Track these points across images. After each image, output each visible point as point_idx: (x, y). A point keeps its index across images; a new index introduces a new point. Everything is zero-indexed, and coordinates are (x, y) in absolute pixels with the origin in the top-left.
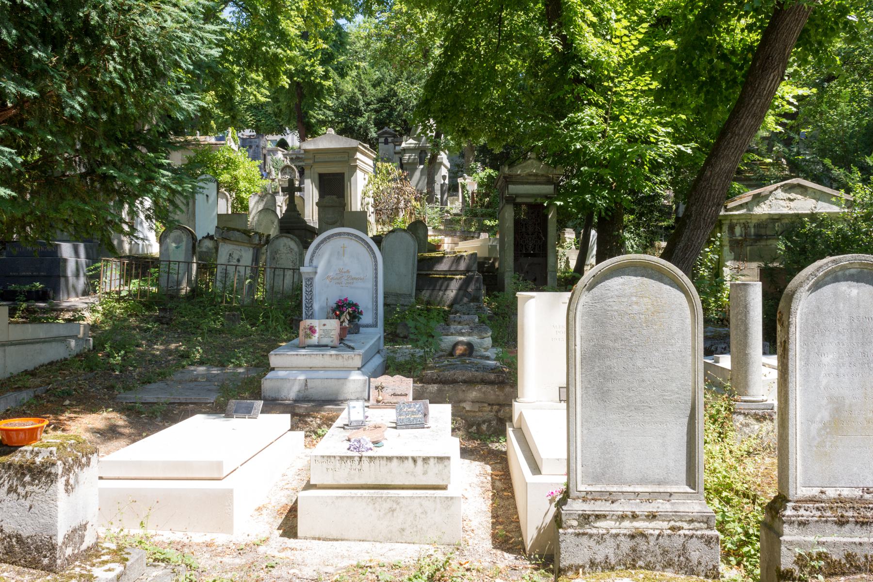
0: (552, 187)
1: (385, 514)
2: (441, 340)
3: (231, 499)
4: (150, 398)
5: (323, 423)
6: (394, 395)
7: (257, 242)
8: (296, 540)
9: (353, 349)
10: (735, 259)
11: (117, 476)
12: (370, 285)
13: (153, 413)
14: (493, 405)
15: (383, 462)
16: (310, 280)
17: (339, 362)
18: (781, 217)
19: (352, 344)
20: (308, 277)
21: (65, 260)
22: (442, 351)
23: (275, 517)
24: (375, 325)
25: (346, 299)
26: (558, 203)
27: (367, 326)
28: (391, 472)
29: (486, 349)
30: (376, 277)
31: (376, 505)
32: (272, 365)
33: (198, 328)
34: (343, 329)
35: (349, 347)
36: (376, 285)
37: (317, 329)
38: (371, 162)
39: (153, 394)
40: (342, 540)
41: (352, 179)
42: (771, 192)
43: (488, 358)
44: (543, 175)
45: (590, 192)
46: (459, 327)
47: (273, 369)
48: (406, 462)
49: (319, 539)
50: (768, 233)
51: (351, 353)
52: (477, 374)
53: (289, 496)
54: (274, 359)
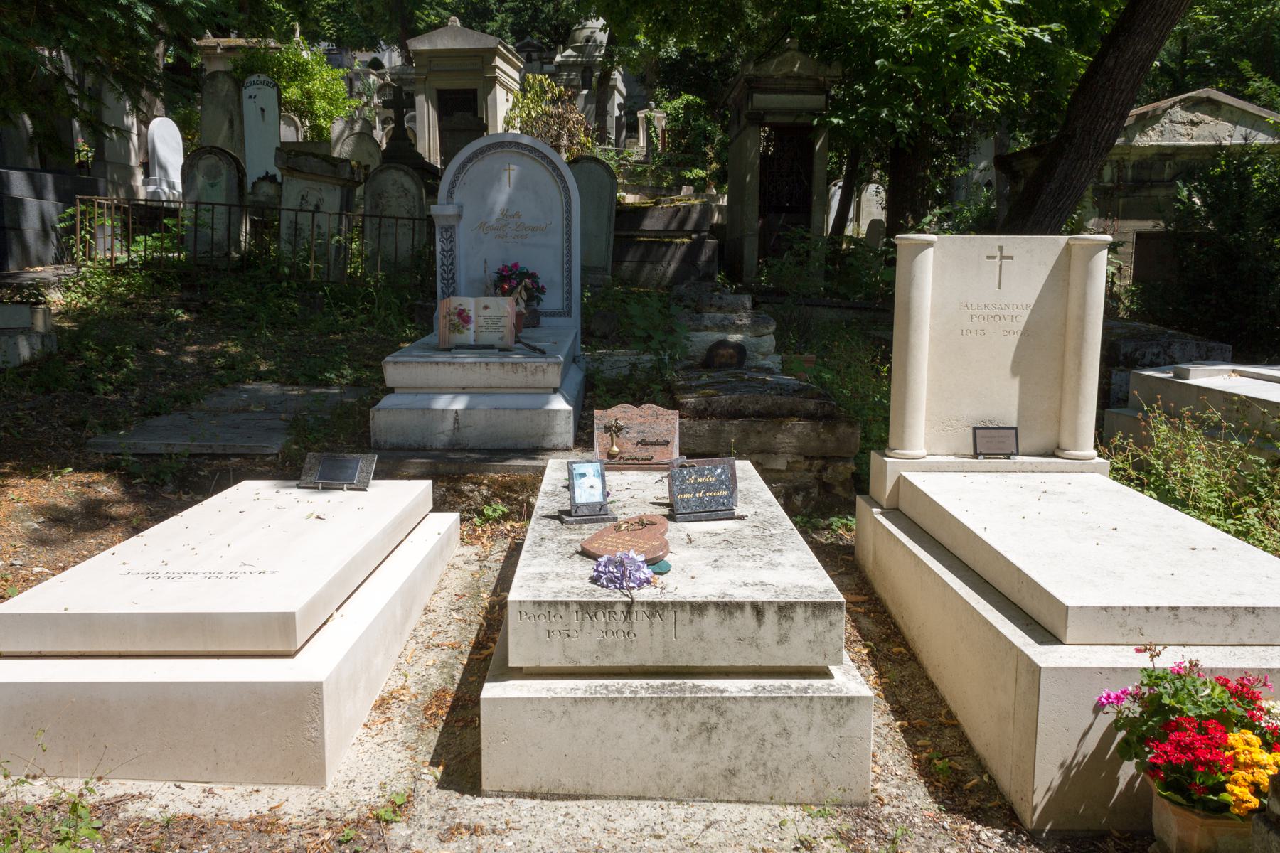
0: (823, 98)
1: (691, 738)
2: (688, 339)
3: (319, 707)
4: (153, 445)
5: (494, 495)
6: (643, 443)
7: (347, 176)
8: (479, 801)
9: (543, 352)
10: (1100, 217)
11: (35, 649)
12: (557, 240)
13: (157, 476)
14: (812, 458)
15: (684, 616)
16: (450, 230)
17: (519, 378)
18: (1179, 150)
19: (539, 345)
20: (444, 223)
21: (19, 203)
22: (688, 358)
23: (421, 728)
24: (568, 313)
25: (516, 265)
26: (835, 121)
27: (553, 314)
28: (701, 637)
29: (765, 355)
30: (569, 226)
31: (671, 718)
32: (389, 383)
33: (251, 319)
34: (519, 315)
35: (535, 349)
36: (569, 241)
37: (472, 314)
38: (516, 75)
39: (165, 438)
40: (588, 797)
41: (489, 97)
42: (1165, 111)
43: (769, 371)
44: (808, 78)
45: (887, 104)
46: (720, 316)
47: (391, 390)
48: (738, 614)
49: (533, 796)
50: (1154, 177)
51: (541, 361)
52: (781, 400)
53: (444, 665)
54: (394, 372)
